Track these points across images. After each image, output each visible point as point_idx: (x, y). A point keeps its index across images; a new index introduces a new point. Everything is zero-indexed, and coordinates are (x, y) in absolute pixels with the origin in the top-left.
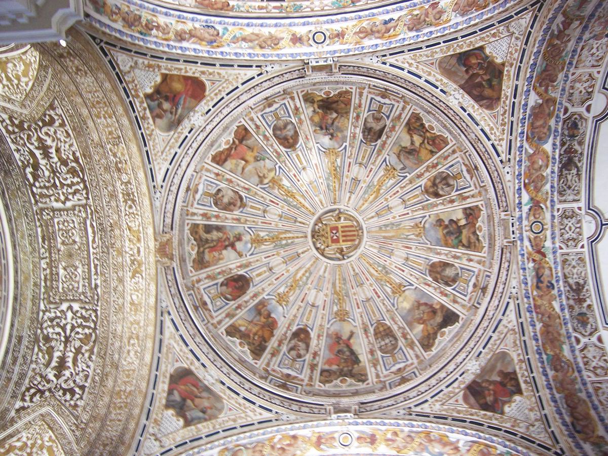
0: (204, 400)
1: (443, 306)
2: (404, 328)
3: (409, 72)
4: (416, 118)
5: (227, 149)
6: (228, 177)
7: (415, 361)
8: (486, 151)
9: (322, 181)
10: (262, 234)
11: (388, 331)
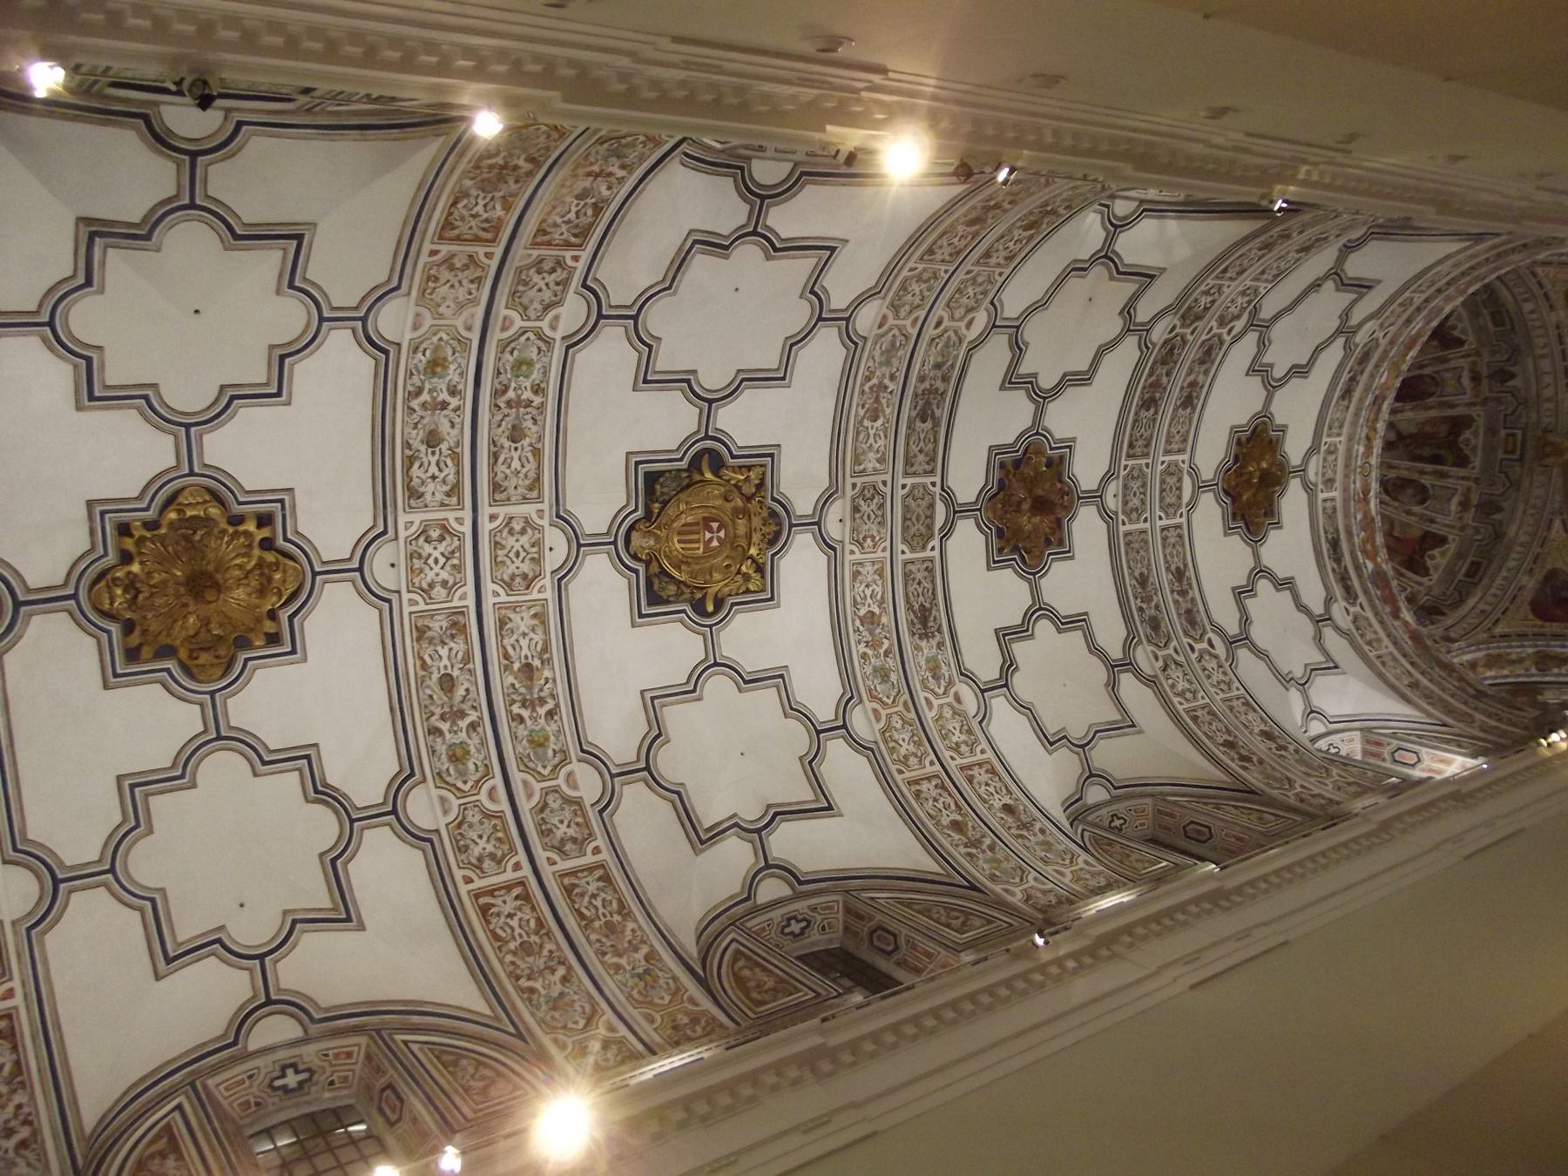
5: (1430, 549)
6: (1412, 518)
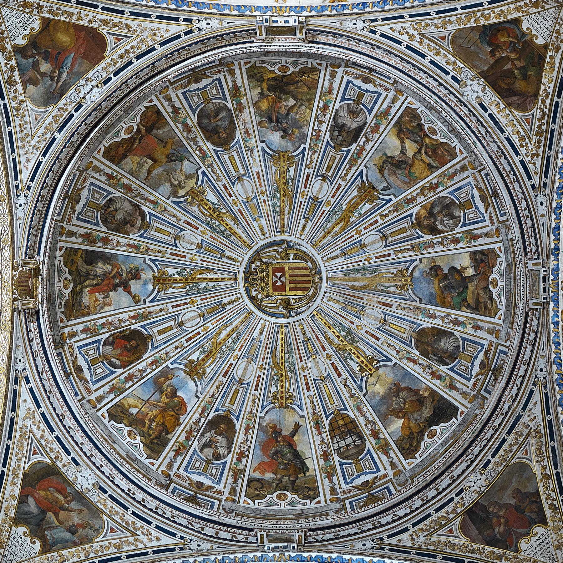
0: (75, 514)
1: (433, 393)
2: (375, 424)
3: (408, 47)
4: (412, 113)
6: (126, 182)
7: (390, 472)
8: (512, 169)
9: (265, 198)
10: (171, 271)
11: (350, 426)
